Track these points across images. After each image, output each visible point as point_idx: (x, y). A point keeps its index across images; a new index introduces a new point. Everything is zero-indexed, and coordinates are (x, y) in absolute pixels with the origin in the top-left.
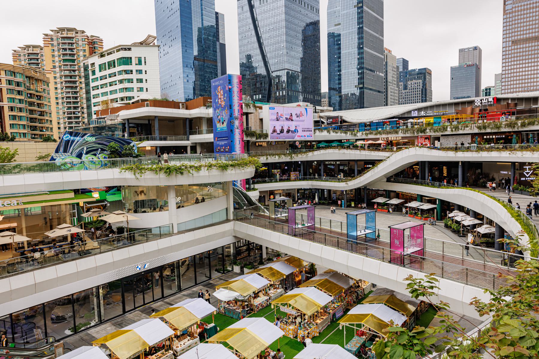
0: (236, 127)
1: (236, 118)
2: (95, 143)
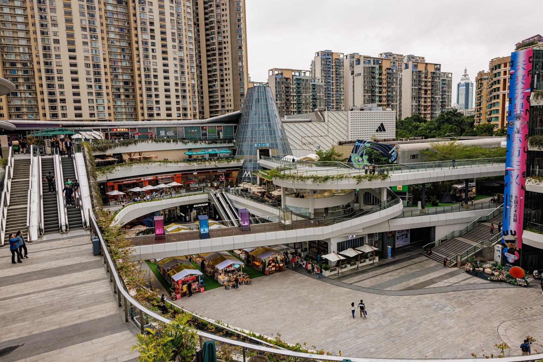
0: (515, 130)
1: (518, 117)
2: (370, 147)
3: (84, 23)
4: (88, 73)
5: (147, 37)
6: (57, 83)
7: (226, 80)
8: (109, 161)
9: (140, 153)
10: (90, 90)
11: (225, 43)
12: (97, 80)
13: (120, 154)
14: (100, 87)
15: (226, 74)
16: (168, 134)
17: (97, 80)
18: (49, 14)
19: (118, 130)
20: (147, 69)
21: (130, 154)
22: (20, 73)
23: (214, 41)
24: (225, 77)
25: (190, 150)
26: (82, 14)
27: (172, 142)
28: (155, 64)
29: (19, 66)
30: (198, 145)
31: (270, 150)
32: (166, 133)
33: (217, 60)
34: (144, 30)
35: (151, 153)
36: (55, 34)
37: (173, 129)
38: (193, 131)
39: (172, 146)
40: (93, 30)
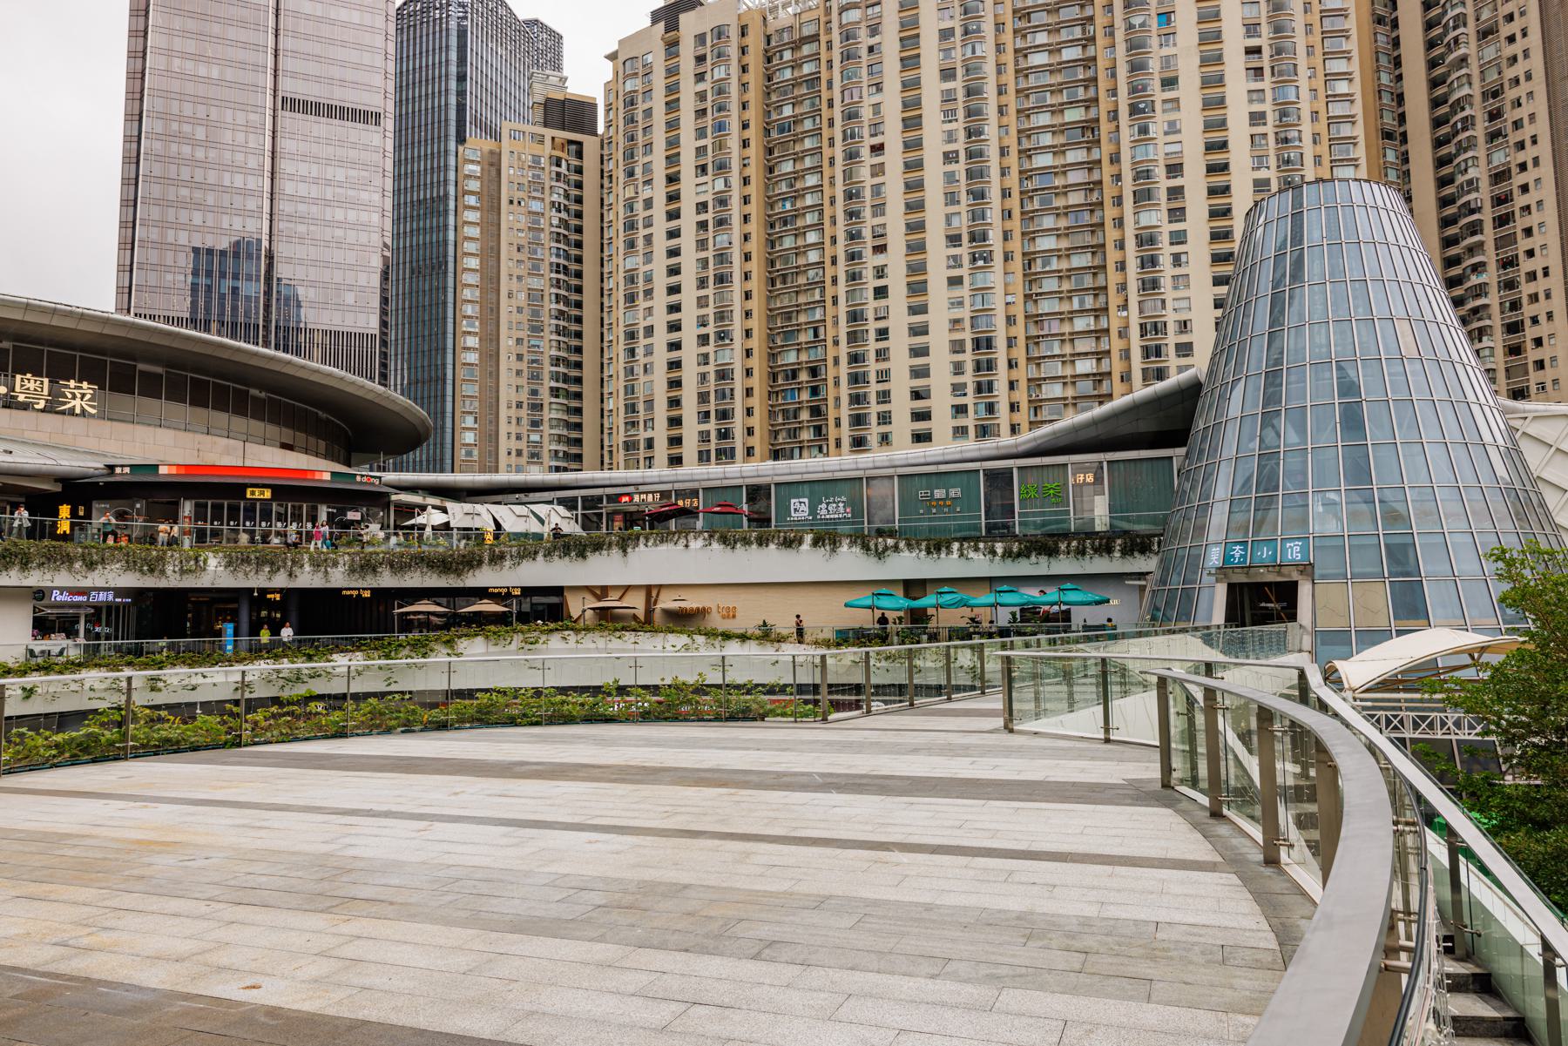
3: (955, 222)
4: (958, 369)
5: (1156, 217)
6: (874, 409)
7: (1535, 320)
8: (480, 613)
9: (651, 592)
10: (961, 422)
11: (1523, 167)
12: (983, 388)
13: (558, 591)
14: (991, 408)
15: (1534, 298)
16: (822, 510)
17: (983, 388)
18: (869, 221)
19: (636, 498)
20: (1151, 328)
21: (602, 592)
22: (805, 396)
23: (1472, 173)
24: (1528, 310)
25: (912, 587)
26: (951, 198)
27: (806, 546)
28: (1184, 304)
29: (804, 376)
30: (950, 565)
31: (1304, 591)
32: (813, 510)
33: (1490, 246)
34: (1143, 197)
35: (684, 594)
36: (880, 272)
37: (846, 486)
38: (939, 493)
39: (808, 562)
40: (978, 237)
